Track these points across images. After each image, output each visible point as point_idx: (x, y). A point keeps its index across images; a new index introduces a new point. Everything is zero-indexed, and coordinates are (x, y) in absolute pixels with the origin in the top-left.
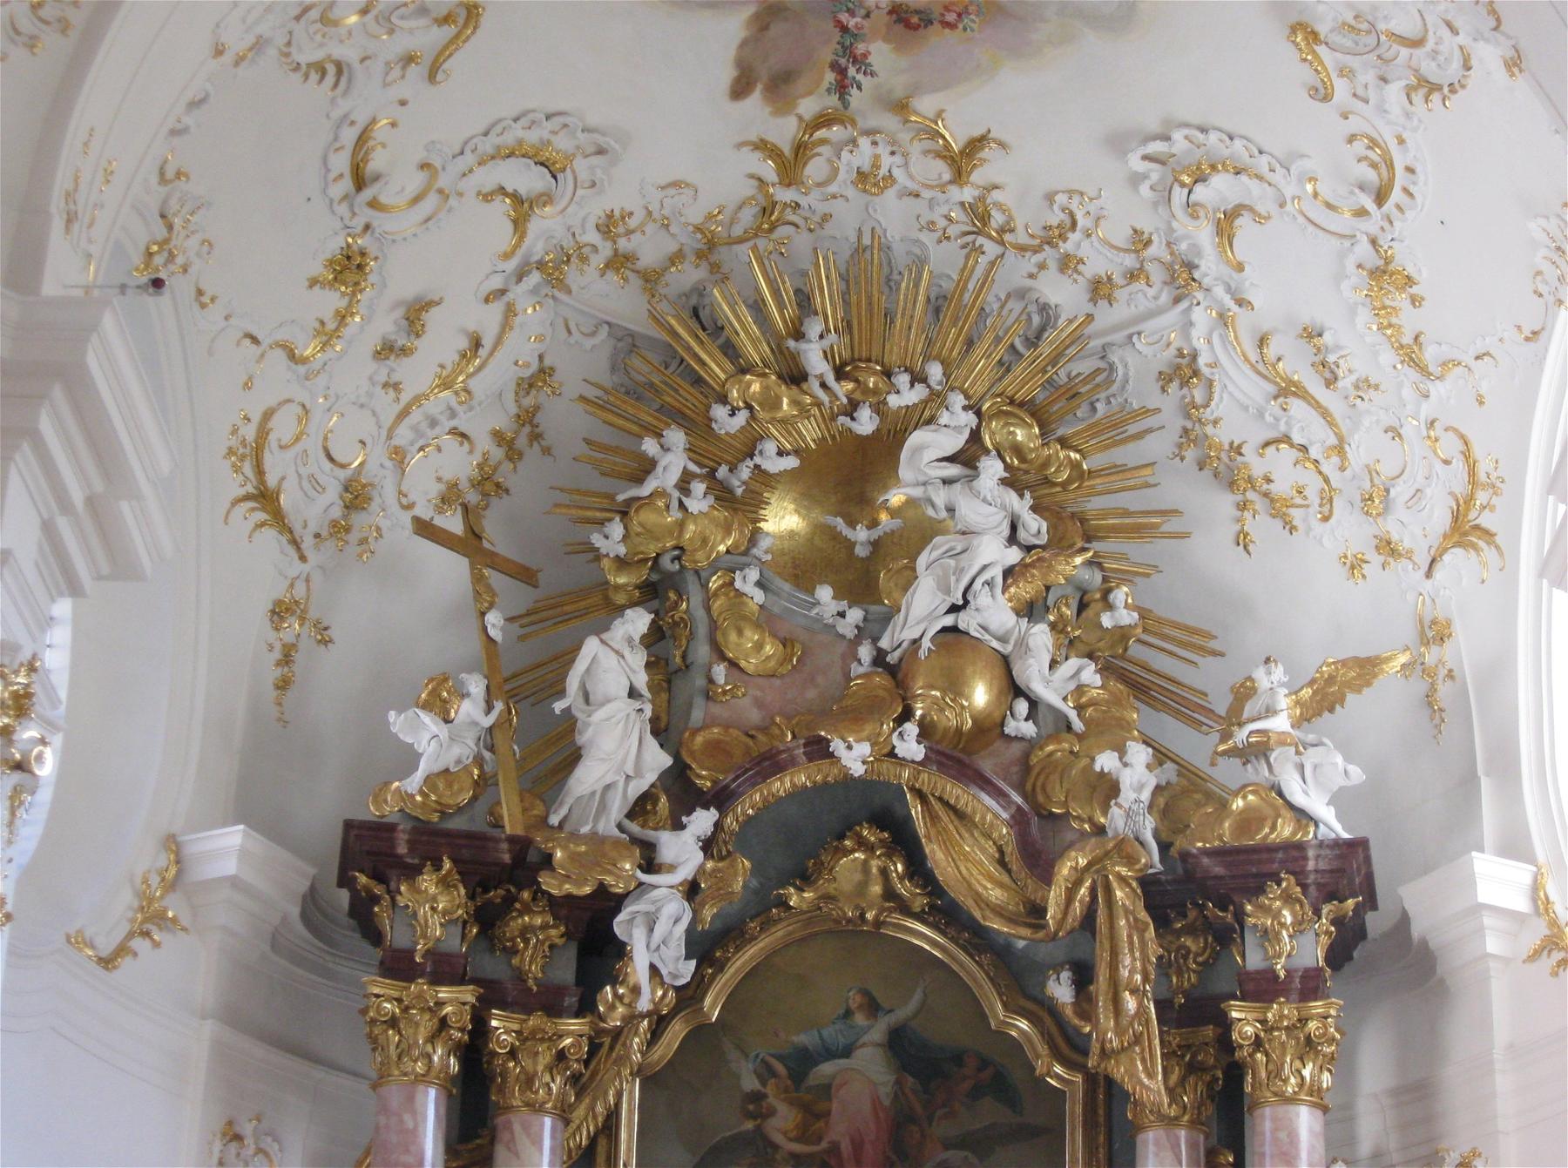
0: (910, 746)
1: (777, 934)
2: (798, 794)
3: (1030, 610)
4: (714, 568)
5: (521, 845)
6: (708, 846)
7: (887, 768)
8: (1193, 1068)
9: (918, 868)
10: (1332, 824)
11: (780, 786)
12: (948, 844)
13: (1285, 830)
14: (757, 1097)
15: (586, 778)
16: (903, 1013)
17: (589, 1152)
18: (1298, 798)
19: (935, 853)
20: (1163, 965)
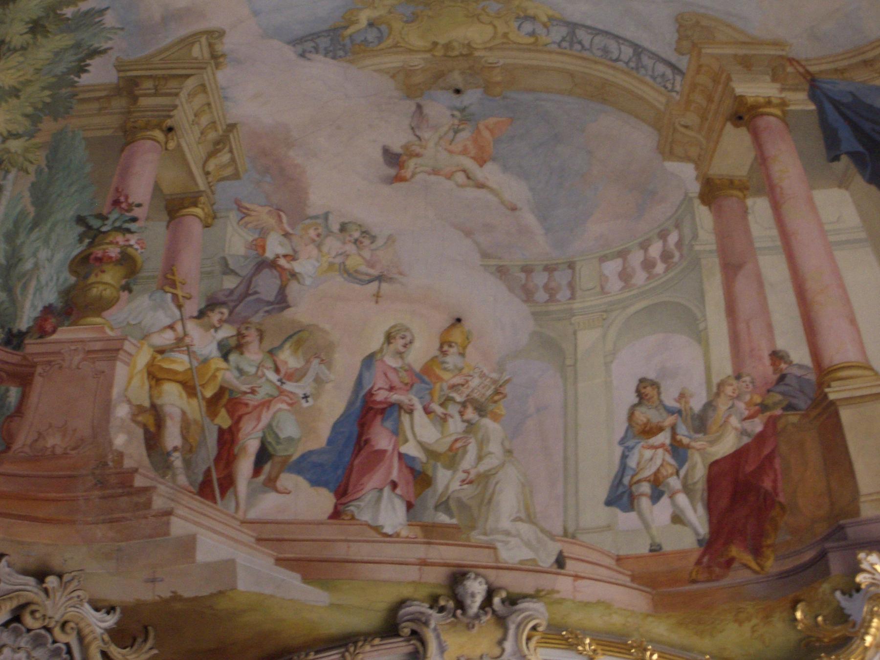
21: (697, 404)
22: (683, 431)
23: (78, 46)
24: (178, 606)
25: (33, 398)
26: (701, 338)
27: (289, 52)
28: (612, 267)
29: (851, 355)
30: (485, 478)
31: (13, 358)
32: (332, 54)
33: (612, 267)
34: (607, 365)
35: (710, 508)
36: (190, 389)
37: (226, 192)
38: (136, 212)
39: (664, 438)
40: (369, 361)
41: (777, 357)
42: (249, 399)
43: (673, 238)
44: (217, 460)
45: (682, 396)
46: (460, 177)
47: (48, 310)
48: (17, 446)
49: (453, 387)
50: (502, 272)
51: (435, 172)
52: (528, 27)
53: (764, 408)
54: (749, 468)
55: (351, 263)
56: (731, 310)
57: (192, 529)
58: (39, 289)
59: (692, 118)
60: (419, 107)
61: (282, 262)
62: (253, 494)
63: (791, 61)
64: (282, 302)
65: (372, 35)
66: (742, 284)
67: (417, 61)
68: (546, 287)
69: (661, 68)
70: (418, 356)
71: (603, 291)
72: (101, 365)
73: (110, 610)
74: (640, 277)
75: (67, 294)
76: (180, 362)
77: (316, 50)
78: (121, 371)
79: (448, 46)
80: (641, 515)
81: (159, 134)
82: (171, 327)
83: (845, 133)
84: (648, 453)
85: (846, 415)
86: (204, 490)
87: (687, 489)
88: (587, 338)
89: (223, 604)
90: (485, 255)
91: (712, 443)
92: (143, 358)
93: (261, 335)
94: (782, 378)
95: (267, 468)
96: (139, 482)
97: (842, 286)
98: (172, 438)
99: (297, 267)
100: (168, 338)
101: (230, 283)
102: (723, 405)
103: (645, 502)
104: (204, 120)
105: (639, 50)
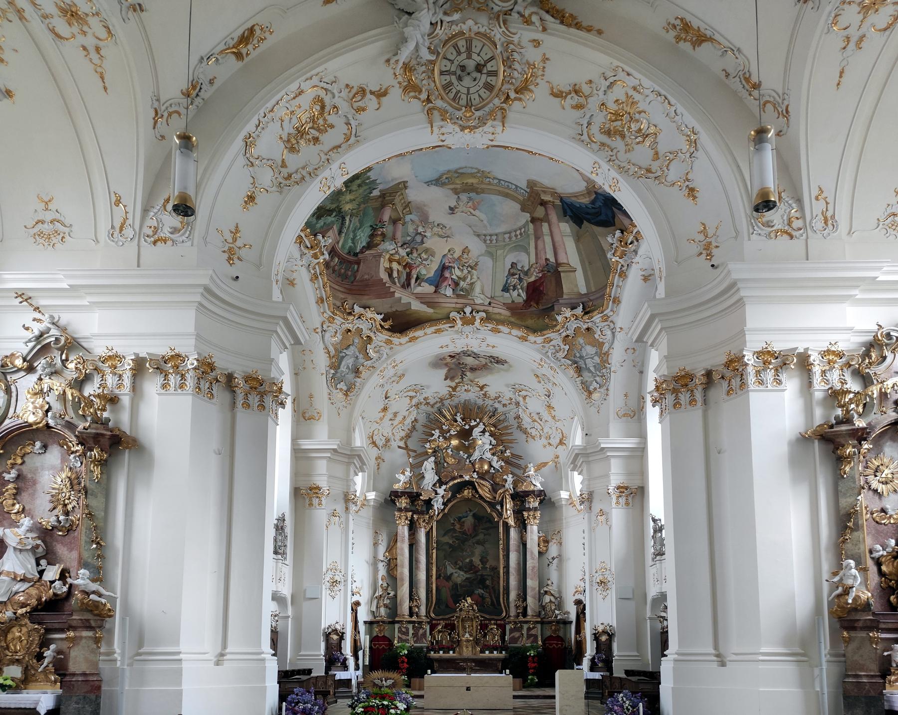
0: (475, 475)
1: (455, 501)
2: (458, 483)
3: (493, 454)
4: (444, 449)
5: (417, 493)
6: (445, 490)
7: (472, 479)
8: (518, 520)
9: (477, 492)
10: (539, 487)
11: (456, 481)
12: (482, 489)
13: (532, 488)
14: (454, 523)
15: (426, 482)
16: (475, 511)
17: (429, 532)
18: (534, 483)
19: (480, 490)
20: (514, 506)
21: (526, 269)
22: (522, 275)
23: (370, 188)
24: (397, 313)
25: (361, 268)
26: (528, 254)
27: (425, 185)
28: (507, 236)
29: (565, 261)
30: (472, 284)
31: (355, 258)
32: (436, 185)
33: (507, 236)
34: (504, 259)
35: (527, 293)
36: (399, 264)
37: (408, 218)
38: (385, 223)
39: (517, 276)
40: (444, 256)
41: (547, 259)
42: (415, 266)
43: (523, 230)
44: (406, 280)
45: (522, 267)
46: (469, 213)
47: (364, 247)
48: (358, 278)
49: (465, 263)
50: (478, 236)
51: (462, 212)
52: (488, 180)
53: (542, 271)
54: (537, 285)
55: (440, 233)
56: (536, 248)
57: (400, 295)
58: (361, 243)
59: (530, 203)
60: (458, 197)
61: (422, 233)
62: (415, 287)
63: (556, 193)
64: (422, 242)
65: (447, 181)
66: (540, 242)
67: (458, 186)
68: (490, 240)
69: (522, 191)
70: (456, 256)
71: (504, 241)
72: (377, 259)
73: (381, 314)
74: (514, 238)
75: (368, 243)
76: (397, 257)
77: (432, 184)
78: (382, 259)
79: (467, 183)
80: (510, 294)
81: (391, 205)
82: (394, 249)
83: (568, 211)
84: (513, 280)
85: (562, 274)
86: (403, 286)
87: (522, 288)
88: (499, 252)
89: (408, 312)
90: (474, 232)
91: (529, 278)
92: (387, 256)
93: (417, 250)
94: (548, 264)
95: (418, 281)
96: (387, 285)
97: (564, 245)
98: (395, 274)
99: (426, 234)
100: (394, 251)
101: (409, 238)
102: (532, 270)
103: (511, 291)
104: (402, 201)
105: (517, 186)
